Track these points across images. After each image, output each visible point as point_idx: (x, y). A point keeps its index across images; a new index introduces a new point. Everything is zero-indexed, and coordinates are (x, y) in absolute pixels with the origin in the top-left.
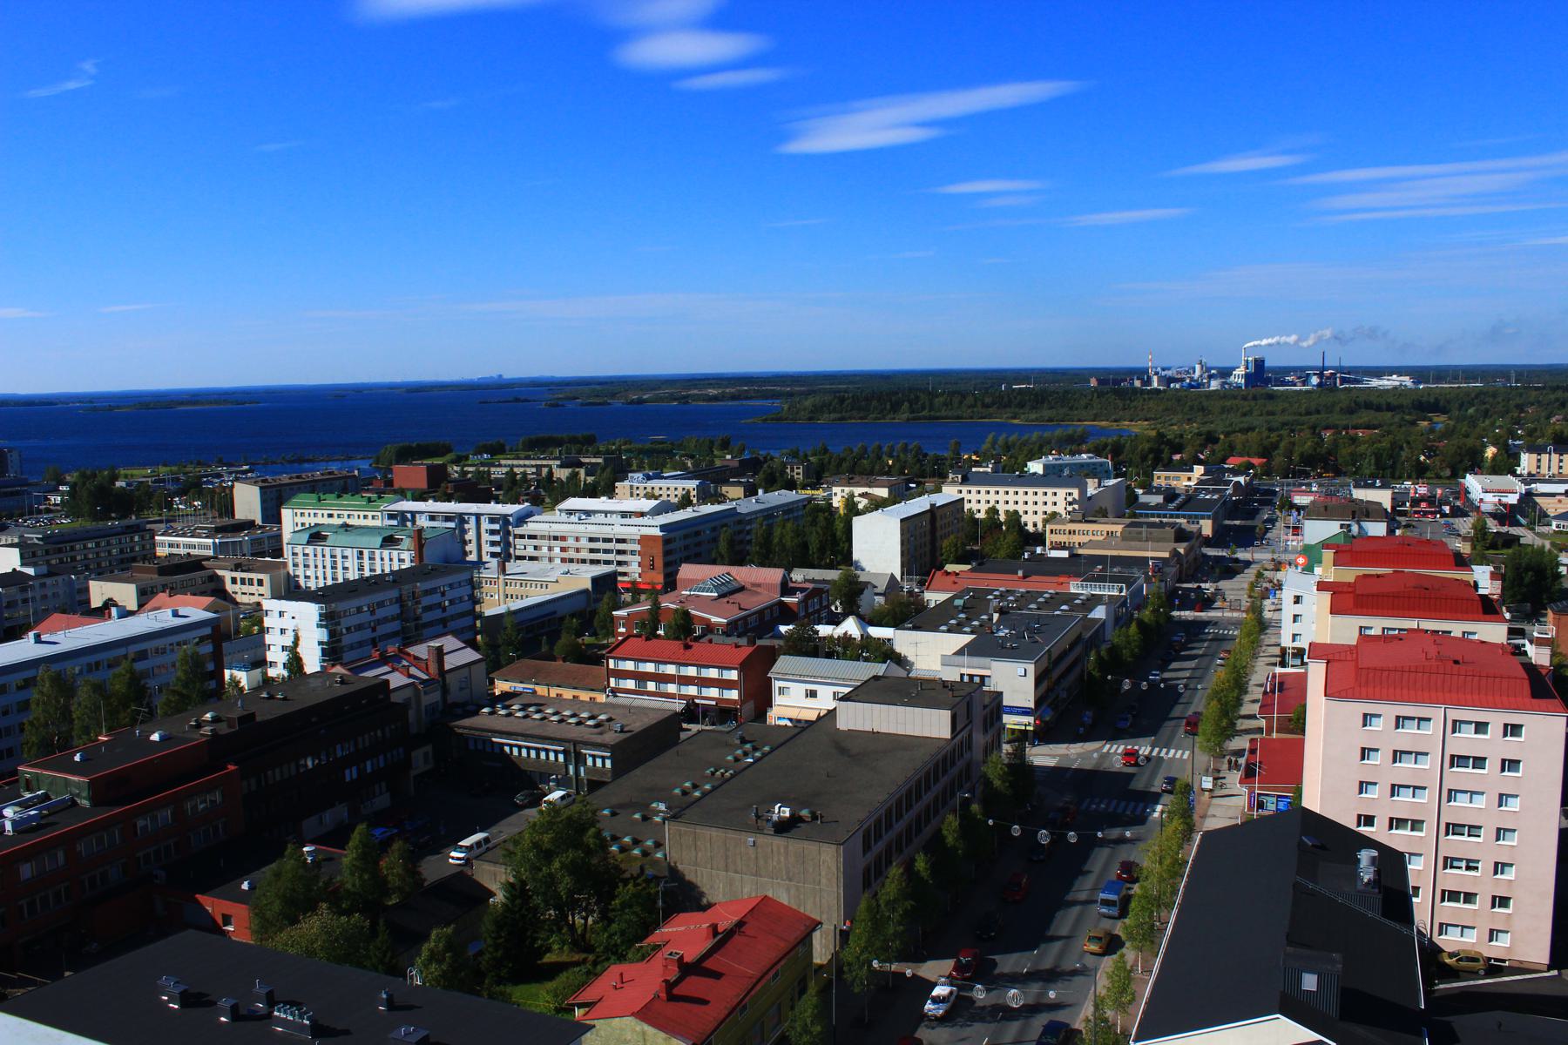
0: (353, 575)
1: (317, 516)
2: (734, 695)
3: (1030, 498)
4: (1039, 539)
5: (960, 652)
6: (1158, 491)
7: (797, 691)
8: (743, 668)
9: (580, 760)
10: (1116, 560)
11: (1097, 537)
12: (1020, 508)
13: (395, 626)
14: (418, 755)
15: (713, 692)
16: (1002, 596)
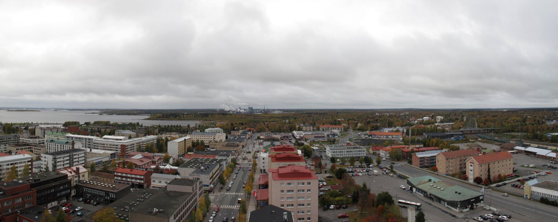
0: (59, 150)
2: (142, 182)
3: (206, 138)
4: (208, 147)
5: (193, 172)
6: (233, 136)
9: (108, 195)
10: (225, 151)
12: (204, 140)
14: (73, 191)
15: (138, 181)
16: (201, 160)
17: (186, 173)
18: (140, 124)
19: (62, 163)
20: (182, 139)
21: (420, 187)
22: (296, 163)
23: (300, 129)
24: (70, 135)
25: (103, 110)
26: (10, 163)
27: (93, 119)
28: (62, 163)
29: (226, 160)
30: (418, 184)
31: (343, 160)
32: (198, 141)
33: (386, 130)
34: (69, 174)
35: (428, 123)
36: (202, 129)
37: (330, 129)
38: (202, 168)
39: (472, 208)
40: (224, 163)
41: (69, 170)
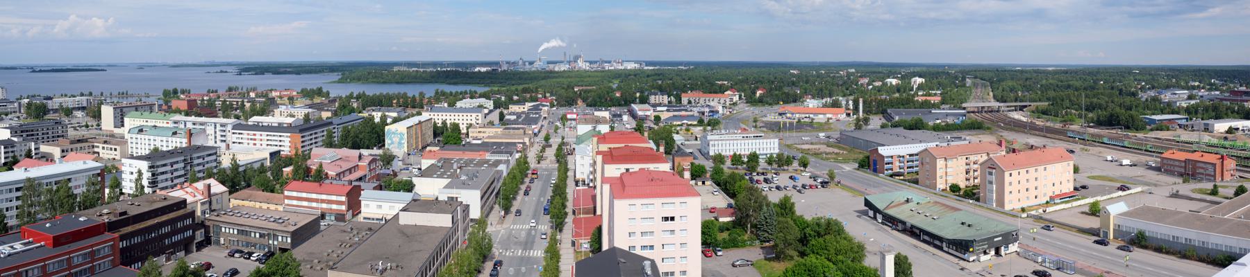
1: (139, 122)
7: (373, 205)
8: (348, 195)
11: (494, 133)
13: (182, 172)
15: (334, 207)
17: (428, 188)
18: (324, 90)
19: (169, 176)
20: (415, 120)
21: (891, 212)
22: (652, 167)
23: (644, 100)
24: (178, 117)
25: (242, 64)
26: (15, 187)
27: (222, 83)
28: (169, 176)
29: (507, 162)
30: (887, 207)
31: (736, 159)
32: (444, 123)
33: (812, 103)
34: (190, 199)
35: (898, 89)
36: (452, 100)
37: (702, 101)
38: (464, 178)
39: (998, 253)
40: (502, 167)
41: (189, 190)
